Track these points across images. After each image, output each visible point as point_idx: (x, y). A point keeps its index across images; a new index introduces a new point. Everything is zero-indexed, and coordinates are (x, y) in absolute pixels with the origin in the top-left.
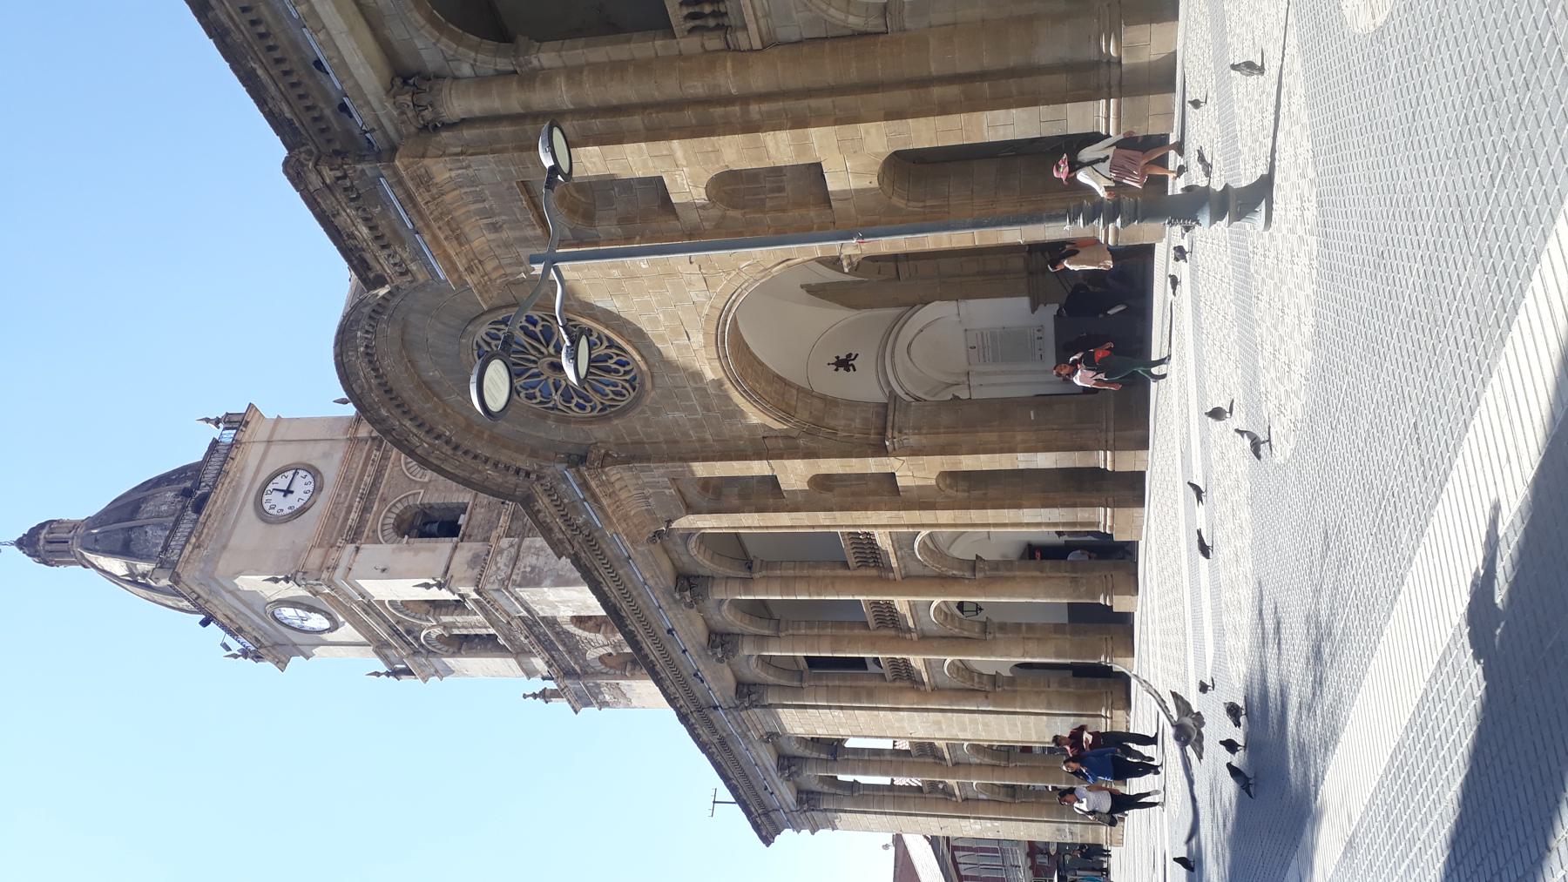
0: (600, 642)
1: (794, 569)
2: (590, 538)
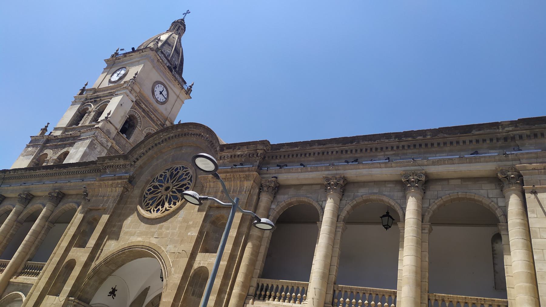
0: (53, 157)
1: (41, 239)
2: (99, 171)
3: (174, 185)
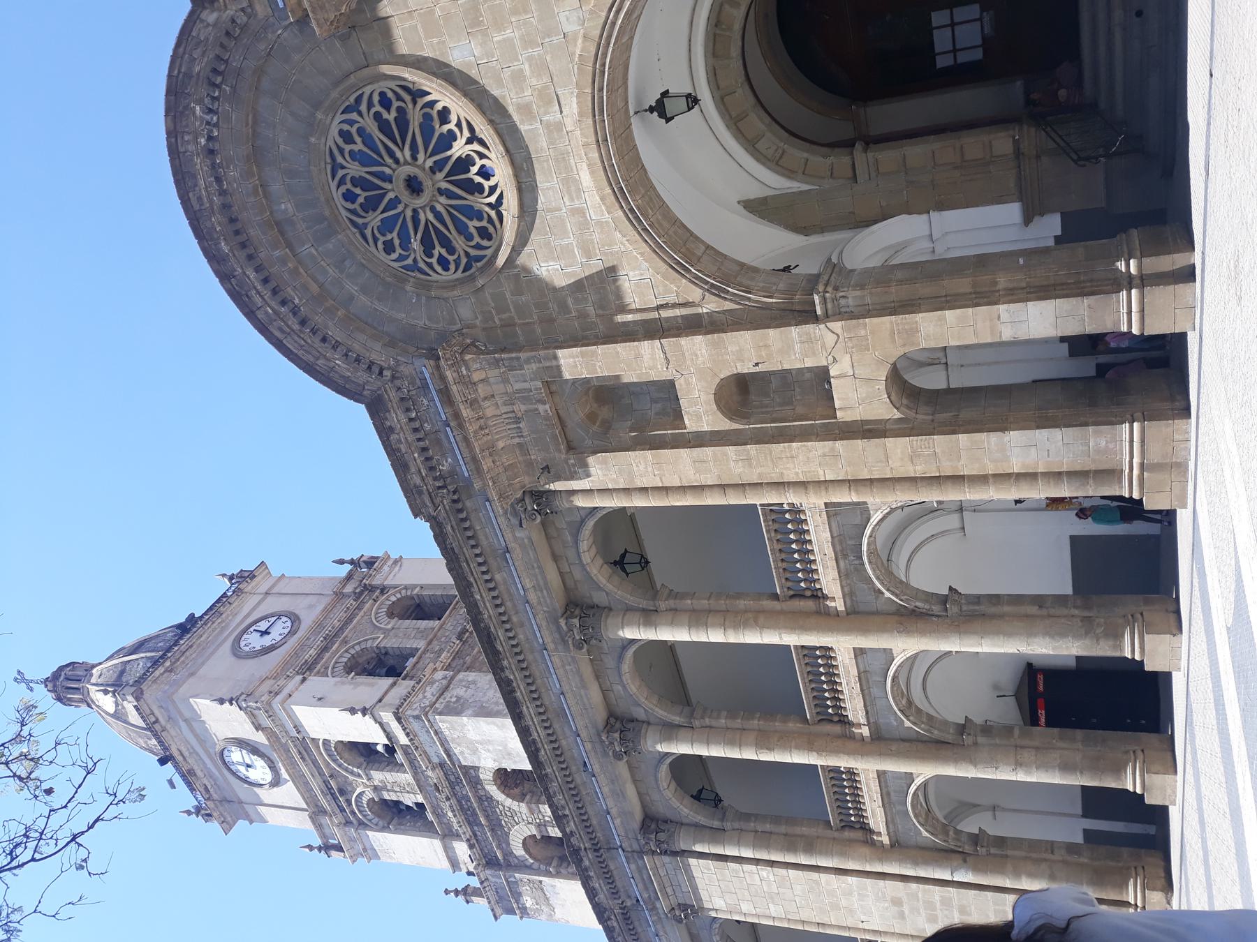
1: (708, 600)
2: (460, 506)
3: (394, 166)
